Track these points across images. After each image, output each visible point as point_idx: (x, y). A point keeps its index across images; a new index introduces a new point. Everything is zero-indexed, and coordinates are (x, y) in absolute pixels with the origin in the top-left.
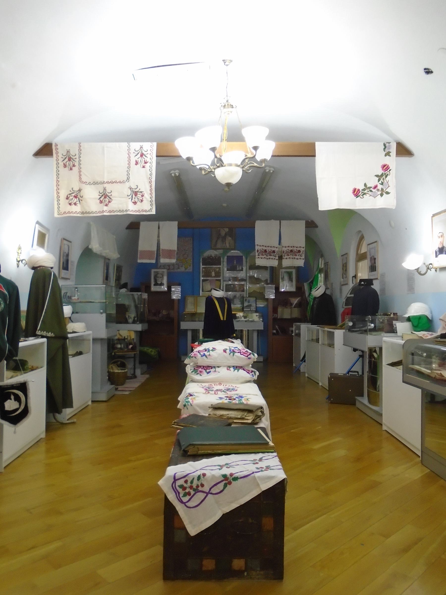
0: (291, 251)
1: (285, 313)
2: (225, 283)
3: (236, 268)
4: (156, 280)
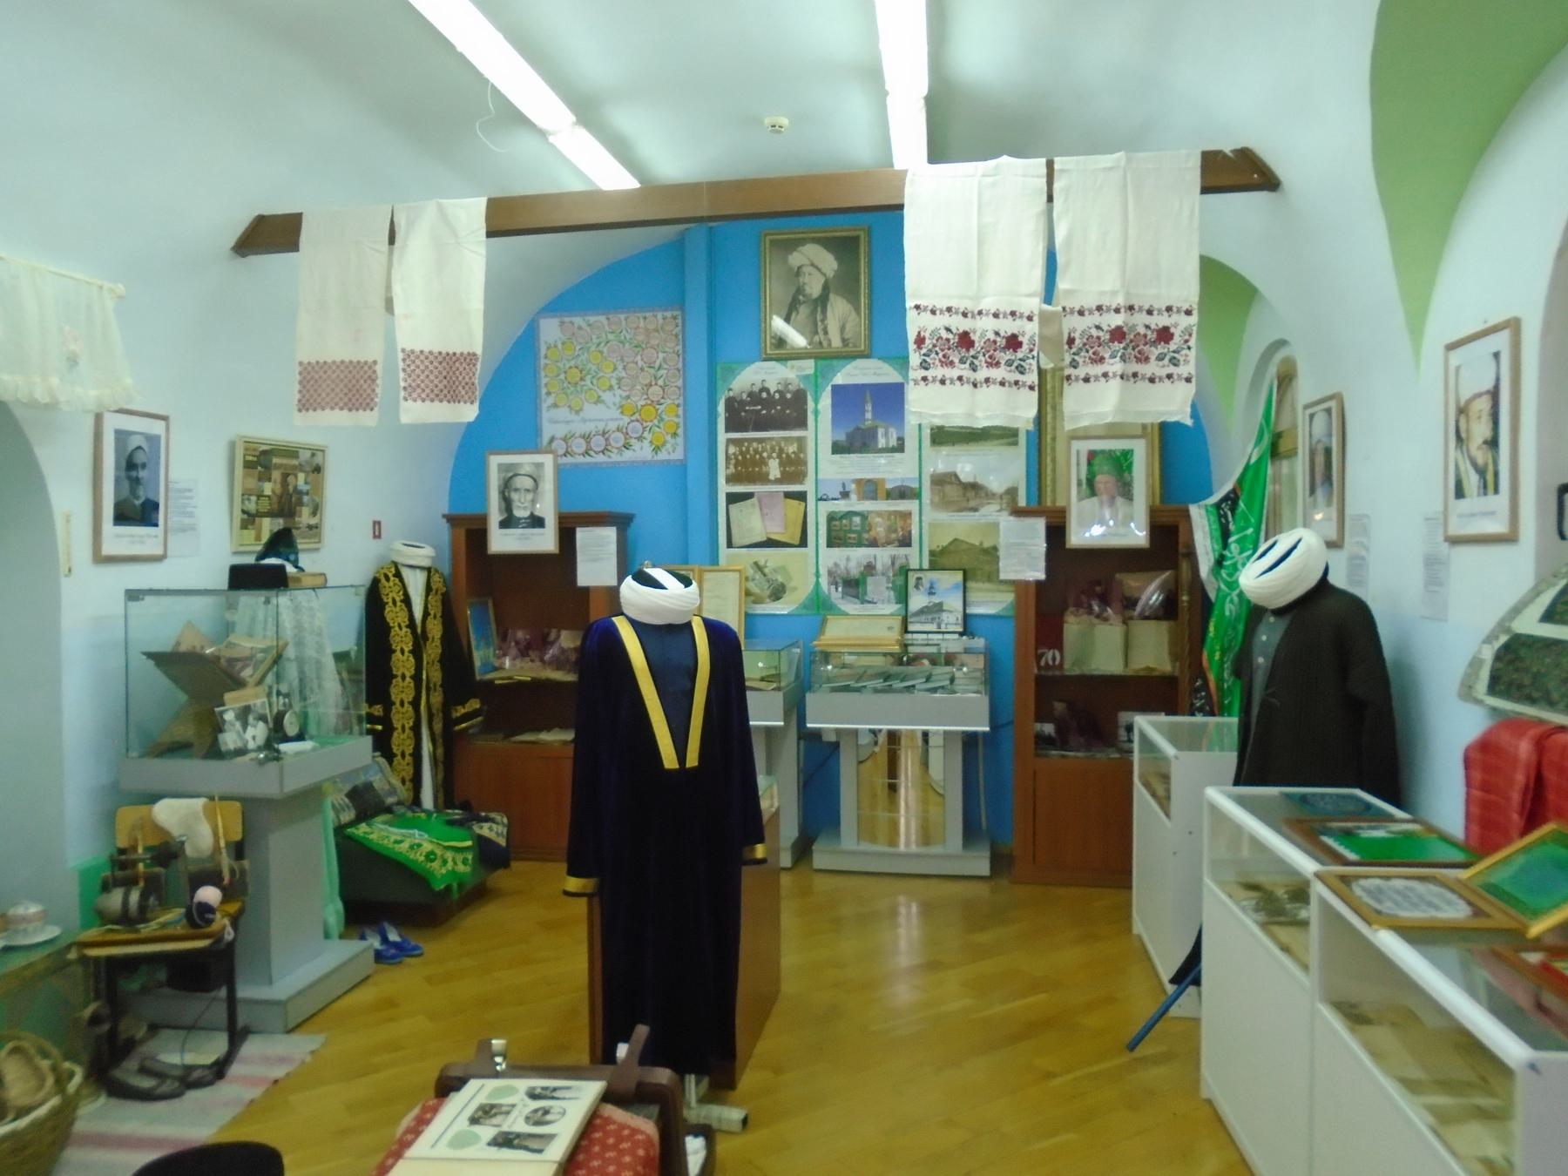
0: (1118, 334)
1: (1102, 646)
2: (826, 508)
3: (874, 437)
4: (507, 504)
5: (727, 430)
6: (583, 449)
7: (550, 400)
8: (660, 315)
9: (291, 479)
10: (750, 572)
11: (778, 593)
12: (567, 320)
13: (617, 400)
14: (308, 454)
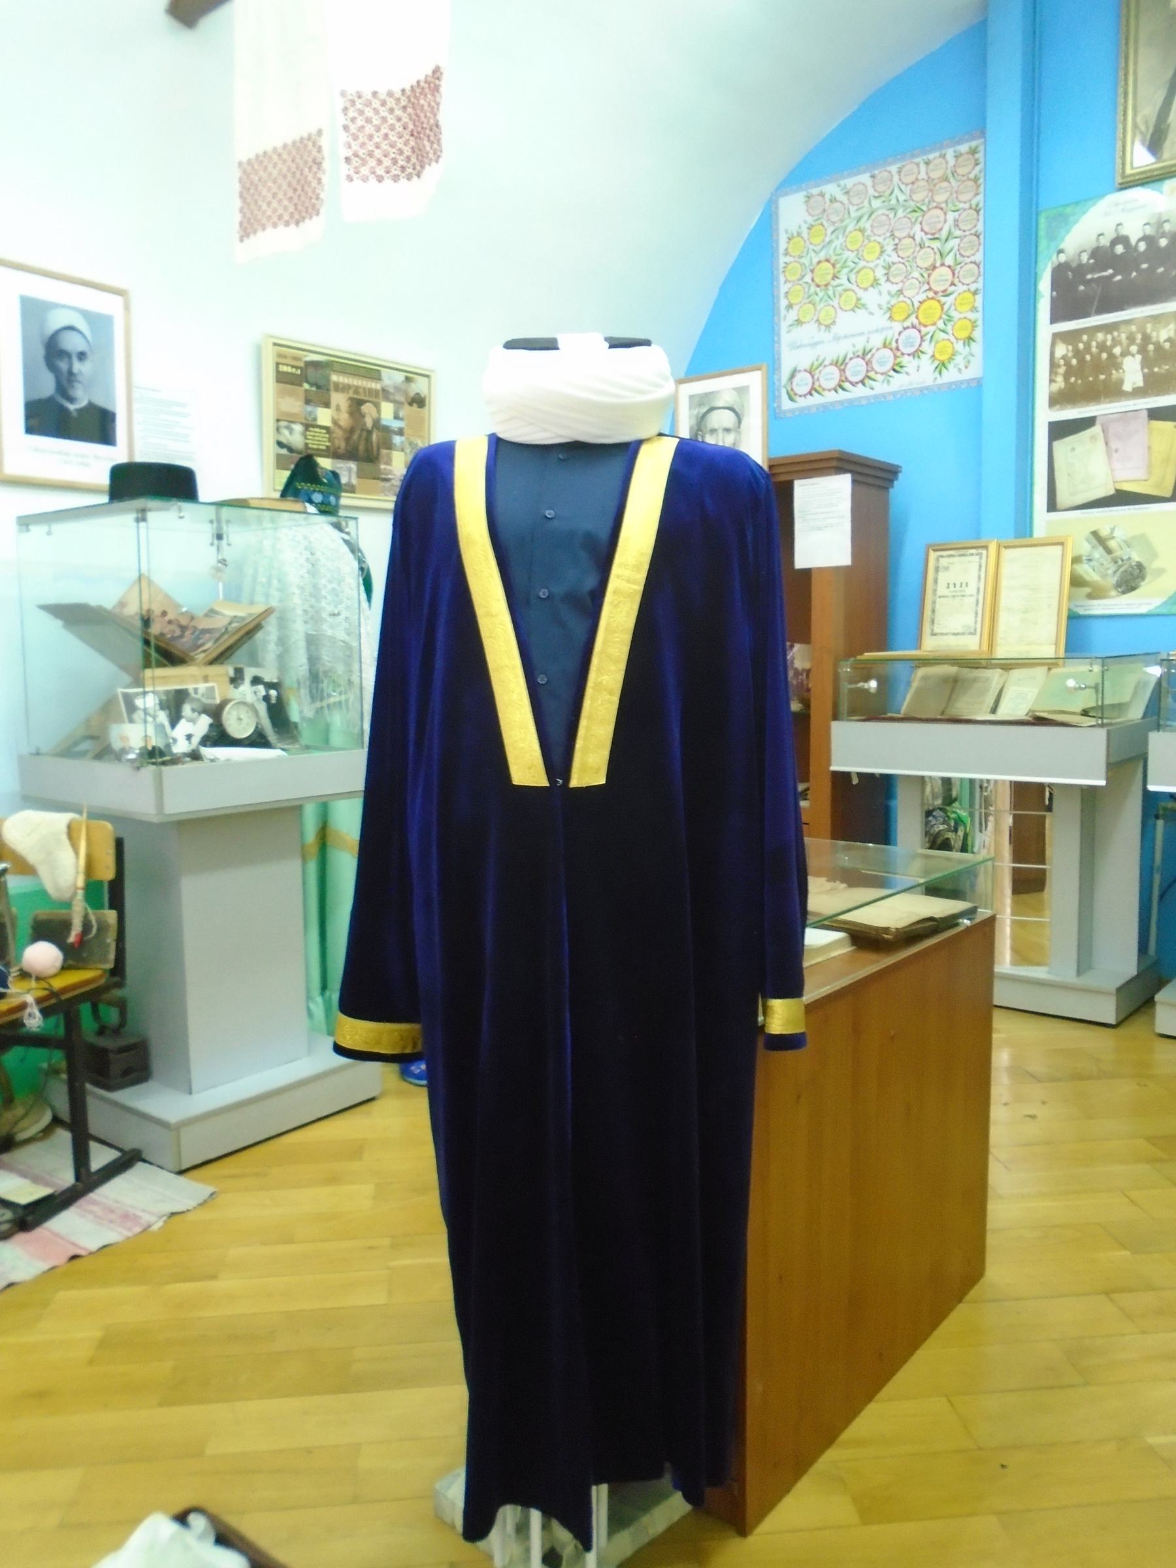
5: (1054, 319)
6: (833, 383)
7: (792, 315)
8: (950, 153)
9: (366, 408)
10: (1085, 548)
11: (1131, 579)
12: (815, 191)
13: (886, 297)
14: (399, 377)
